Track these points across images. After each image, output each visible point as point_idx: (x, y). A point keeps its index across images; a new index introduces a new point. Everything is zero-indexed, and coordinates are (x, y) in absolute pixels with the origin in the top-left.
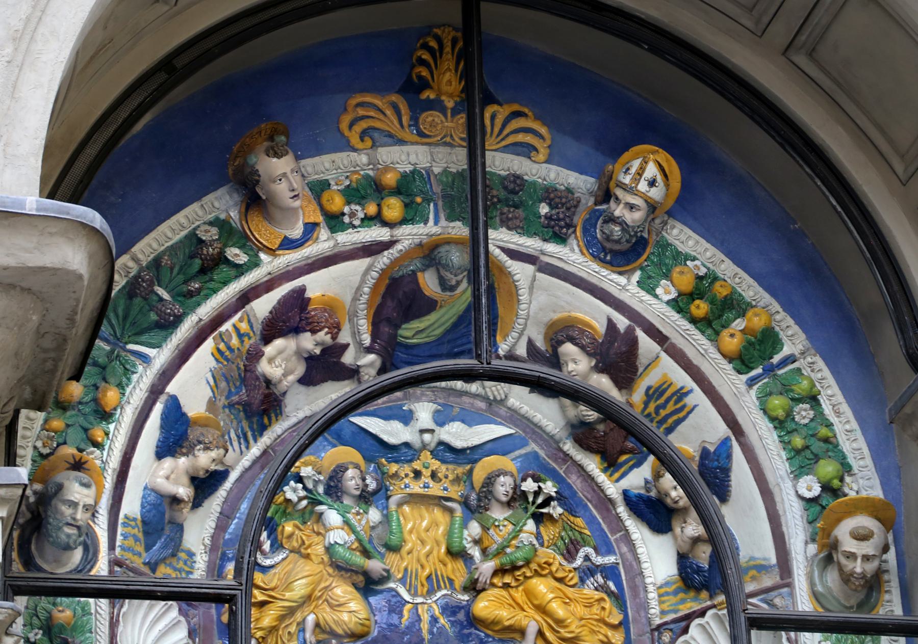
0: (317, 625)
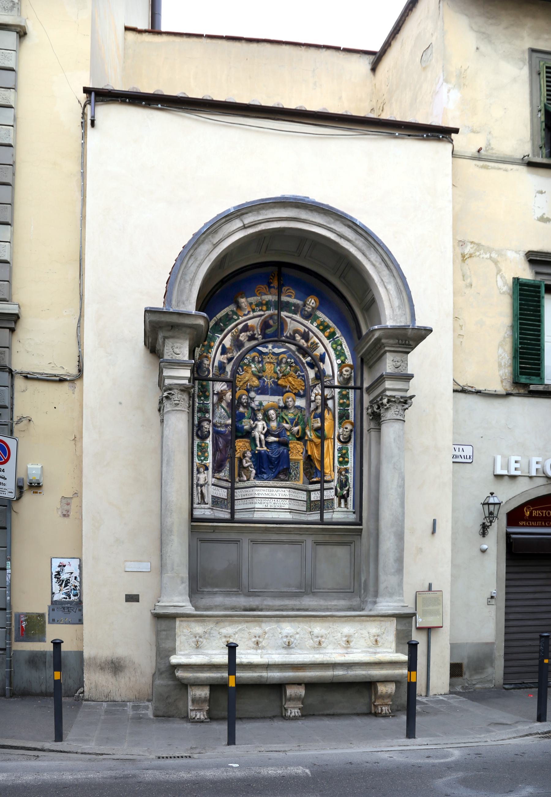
0: (250, 385)
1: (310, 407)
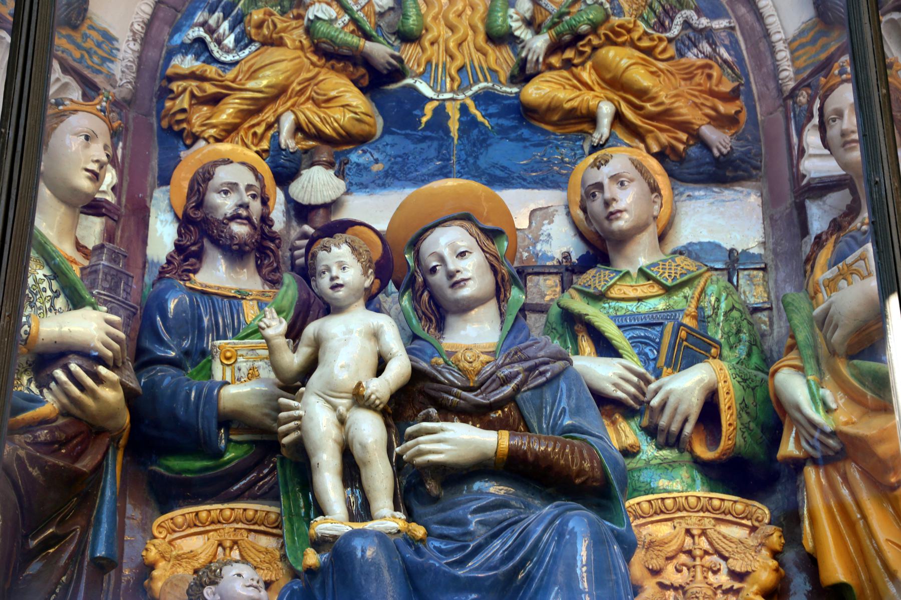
0: (298, 128)
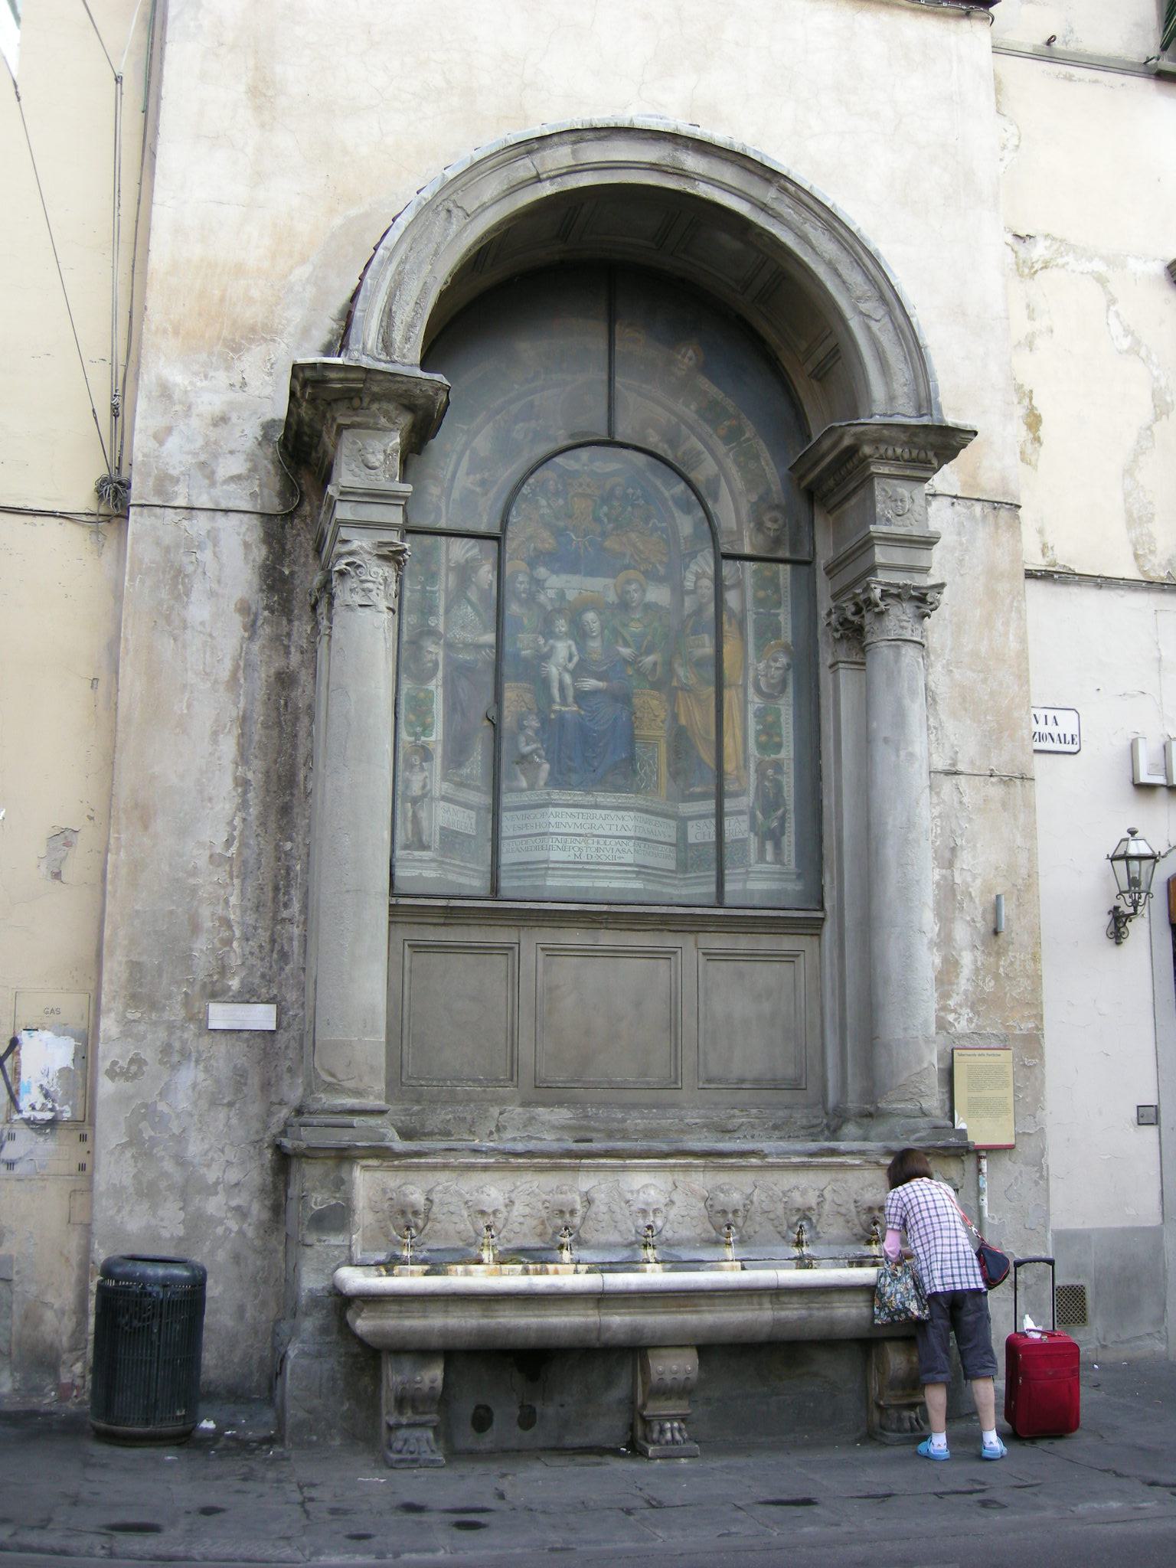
1: (683, 605)
